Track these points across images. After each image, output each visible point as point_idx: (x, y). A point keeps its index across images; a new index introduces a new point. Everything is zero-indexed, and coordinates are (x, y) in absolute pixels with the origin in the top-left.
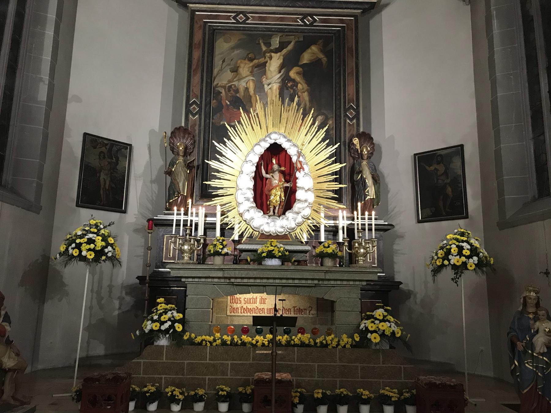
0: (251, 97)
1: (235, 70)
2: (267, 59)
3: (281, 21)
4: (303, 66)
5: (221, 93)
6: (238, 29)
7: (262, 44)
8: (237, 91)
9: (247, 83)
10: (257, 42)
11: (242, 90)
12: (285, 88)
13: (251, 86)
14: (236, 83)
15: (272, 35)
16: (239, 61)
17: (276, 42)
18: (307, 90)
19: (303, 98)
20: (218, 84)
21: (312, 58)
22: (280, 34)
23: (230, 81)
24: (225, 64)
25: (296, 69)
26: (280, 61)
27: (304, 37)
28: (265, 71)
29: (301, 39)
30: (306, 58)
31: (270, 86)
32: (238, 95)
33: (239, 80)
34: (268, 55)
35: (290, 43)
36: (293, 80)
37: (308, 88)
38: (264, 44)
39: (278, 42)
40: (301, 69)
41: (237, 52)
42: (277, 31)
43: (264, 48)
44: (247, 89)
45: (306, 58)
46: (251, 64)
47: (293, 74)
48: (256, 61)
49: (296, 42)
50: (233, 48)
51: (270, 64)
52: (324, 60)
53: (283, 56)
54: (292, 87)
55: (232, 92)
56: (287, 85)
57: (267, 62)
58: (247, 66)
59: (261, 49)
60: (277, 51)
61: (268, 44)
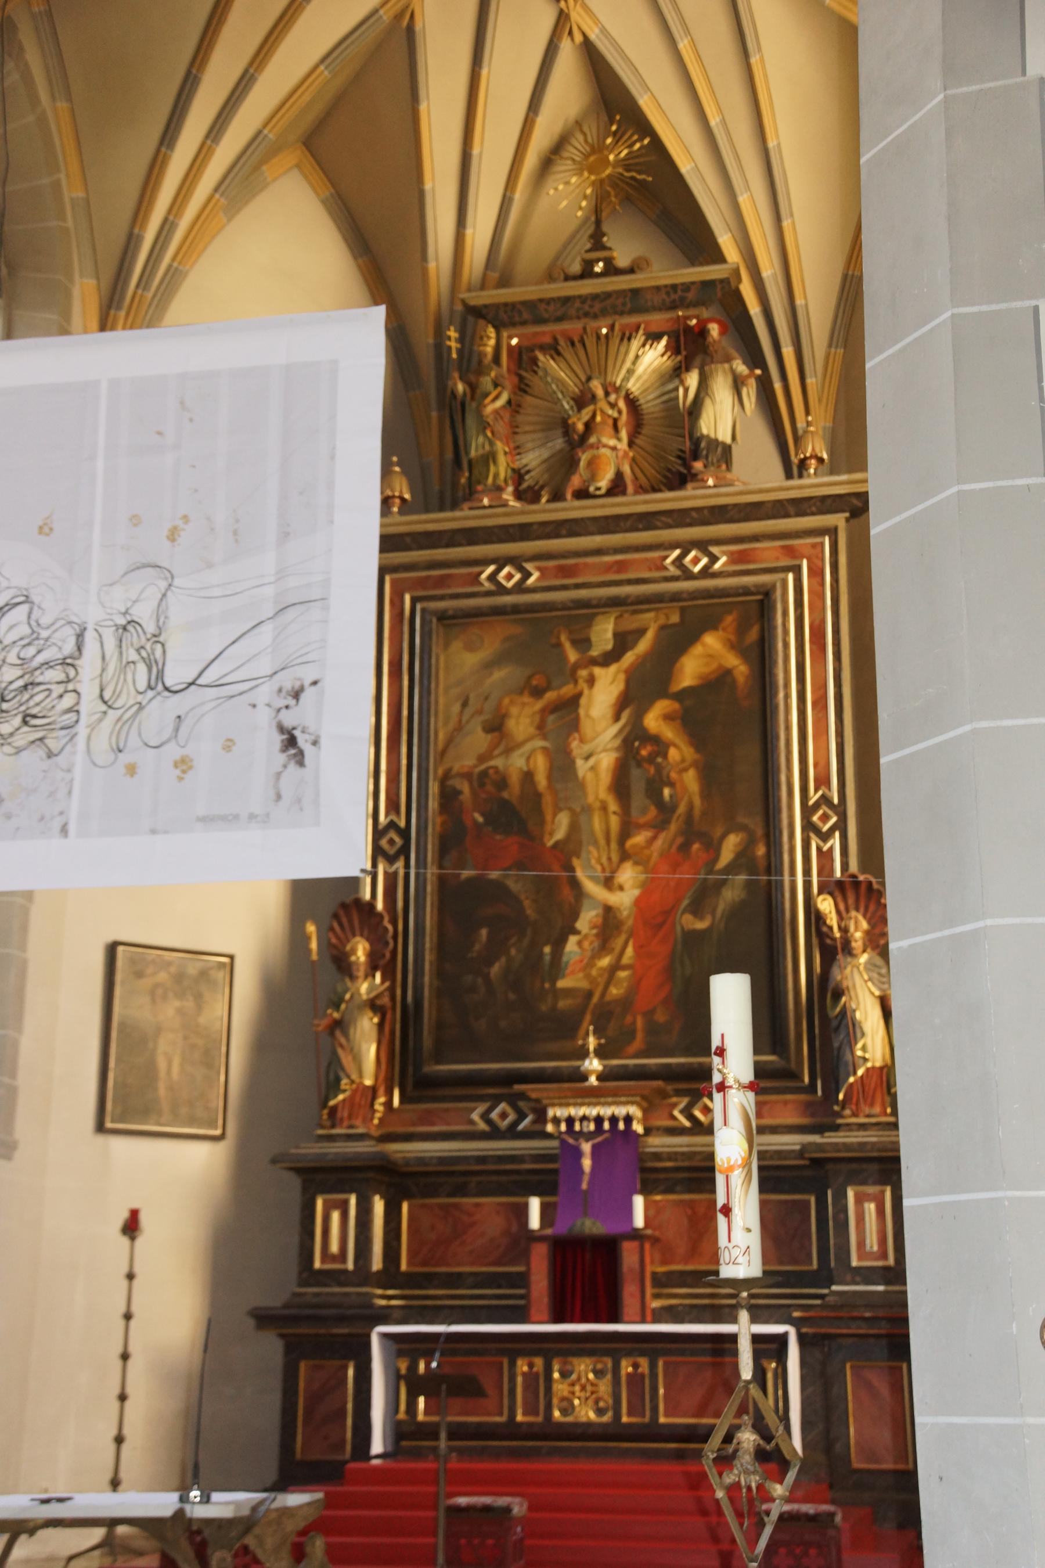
0: (539, 796)
1: (496, 726)
2: (582, 685)
3: (618, 571)
5: (460, 792)
6: (498, 611)
7: (567, 645)
8: (502, 782)
9: (528, 759)
10: (554, 641)
11: (515, 779)
12: (633, 763)
13: (541, 765)
14: (498, 762)
15: (595, 615)
16: (506, 701)
17: (604, 633)
18: (695, 764)
19: (685, 789)
20: (450, 769)
21: (706, 670)
22: (615, 612)
23: (482, 758)
24: (469, 711)
25: (662, 706)
26: (618, 687)
27: (683, 610)
28: (577, 719)
29: (675, 618)
30: (690, 670)
31: (591, 762)
32: (505, 795)
33: (508, 751)
34: (583, 673)
35: (641, 632)
36: (655, 740)
37: (696, 756)
38: (575, 643)
39: (610, 635)
40: (676, 706)
41: (499, 675)
42: (606, 605)
43: (573, 656)
44: (528, 776)
45: (690, 670)
46: (539, 705)
47: (653, 721)
48: (550, 696)
49: (663, 628)
50: (488, 666)
51: (590, 698)
52: (740, 668)
53: (626, 671)
54: (651, 759)
55: (489, 788)
56: (638, 752)
57: (579, 695)
58: (528, 711)
59: (563, 657)
61: (583, 643)
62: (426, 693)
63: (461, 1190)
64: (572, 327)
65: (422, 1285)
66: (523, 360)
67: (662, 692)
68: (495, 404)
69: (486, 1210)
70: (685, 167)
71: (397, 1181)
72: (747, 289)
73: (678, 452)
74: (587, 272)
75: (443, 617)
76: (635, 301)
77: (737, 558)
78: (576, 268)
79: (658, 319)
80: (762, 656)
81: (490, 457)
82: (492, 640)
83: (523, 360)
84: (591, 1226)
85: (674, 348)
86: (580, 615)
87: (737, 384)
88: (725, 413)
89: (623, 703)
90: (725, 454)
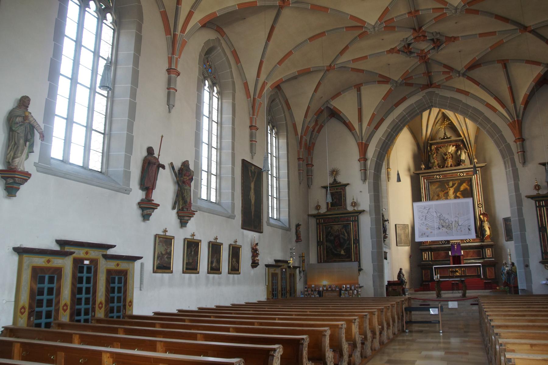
4: (461, 191)
17: (451, 184)
30: (462, 188)
45: (462, 188)
47: (458, 194)
52: (468, 188)
60: (452, 187)
61: (448, 185)
64: (443, 145)
65: (436, 262)
66: (437, 149)
68: (435, 156)
69: (442, 253)
71: (431, 250)
72: (464, 140)
73: (458, 162)
74: (444, 138)
75: (430, 182)
76: (451, 142)
78: (442, 137)
79: (454, 143)
80: (471, 186)
81: (435, 162)
83: (437, 149)
84: (457, 254)
85: (456, 147)
87: (465, 152)
88: (464, 156)
89: (454, 192)
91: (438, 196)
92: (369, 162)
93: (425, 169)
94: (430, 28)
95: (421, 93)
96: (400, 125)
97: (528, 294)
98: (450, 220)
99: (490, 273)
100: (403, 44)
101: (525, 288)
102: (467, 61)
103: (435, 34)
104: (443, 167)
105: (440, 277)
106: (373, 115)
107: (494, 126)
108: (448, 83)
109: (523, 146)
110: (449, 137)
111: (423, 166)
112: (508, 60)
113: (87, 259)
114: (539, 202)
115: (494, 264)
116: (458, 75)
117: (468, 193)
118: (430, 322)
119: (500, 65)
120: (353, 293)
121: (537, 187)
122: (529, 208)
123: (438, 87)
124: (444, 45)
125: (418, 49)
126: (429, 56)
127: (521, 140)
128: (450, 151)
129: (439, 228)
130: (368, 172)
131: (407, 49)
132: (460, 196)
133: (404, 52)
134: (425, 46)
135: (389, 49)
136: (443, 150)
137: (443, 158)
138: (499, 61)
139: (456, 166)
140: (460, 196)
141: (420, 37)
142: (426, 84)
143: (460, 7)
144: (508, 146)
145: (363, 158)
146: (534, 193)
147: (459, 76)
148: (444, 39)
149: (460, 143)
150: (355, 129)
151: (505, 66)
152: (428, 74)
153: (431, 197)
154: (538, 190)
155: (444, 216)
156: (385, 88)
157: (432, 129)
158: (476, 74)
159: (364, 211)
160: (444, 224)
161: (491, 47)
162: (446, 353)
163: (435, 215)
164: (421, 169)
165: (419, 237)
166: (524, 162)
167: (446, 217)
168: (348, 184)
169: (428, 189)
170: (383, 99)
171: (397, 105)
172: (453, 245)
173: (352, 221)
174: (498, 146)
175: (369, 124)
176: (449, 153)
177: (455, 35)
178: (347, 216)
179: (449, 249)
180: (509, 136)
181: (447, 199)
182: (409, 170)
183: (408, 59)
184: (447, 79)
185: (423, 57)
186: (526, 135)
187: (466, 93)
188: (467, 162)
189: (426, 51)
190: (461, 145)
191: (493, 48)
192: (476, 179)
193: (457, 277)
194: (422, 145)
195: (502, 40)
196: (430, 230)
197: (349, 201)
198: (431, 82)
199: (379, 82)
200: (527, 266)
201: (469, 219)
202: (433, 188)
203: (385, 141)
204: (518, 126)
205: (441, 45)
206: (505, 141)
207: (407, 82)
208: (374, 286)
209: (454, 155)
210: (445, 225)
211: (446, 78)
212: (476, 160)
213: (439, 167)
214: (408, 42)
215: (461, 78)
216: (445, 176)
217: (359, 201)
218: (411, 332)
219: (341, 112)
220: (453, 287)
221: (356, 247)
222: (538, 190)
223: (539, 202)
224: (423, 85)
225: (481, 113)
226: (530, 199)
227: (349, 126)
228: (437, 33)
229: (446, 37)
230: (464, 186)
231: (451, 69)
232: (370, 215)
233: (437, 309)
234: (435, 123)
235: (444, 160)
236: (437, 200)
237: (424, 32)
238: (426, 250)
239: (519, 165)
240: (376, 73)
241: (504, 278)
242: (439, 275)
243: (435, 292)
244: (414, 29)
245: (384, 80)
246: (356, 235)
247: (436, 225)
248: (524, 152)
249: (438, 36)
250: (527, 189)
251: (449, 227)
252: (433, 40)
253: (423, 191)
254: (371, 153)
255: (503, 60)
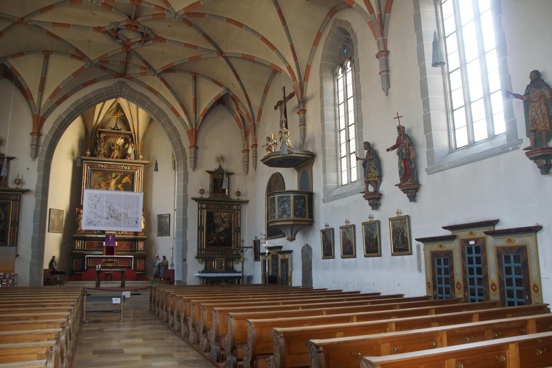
17: (114, 175)
30: (124, 181)
41: (100, 178)
45: (124, 181)
47: (119, 186)
52: (130, 181)
60: (114, 178)
61: (111, 176)
62: (91, 179)
63: (92, 240)
66: (105, 138)
67: (120, 183)
68: (102, 144)
70: (128, 118)
71: (85, 239)
72: (133, 135)
73: (125, 155)
74: (114, 129)
75: (93, 170)
76: (120, 134)
77: (131, 168)
79: (123, 136)
80: (133, 180)
81: (101, 151)
82: (99, 174)
84: (111, 245)
85: (125, 140)
86: (111, 173)
87: (132, 147)
88: (130, 151)
89: (115, 184)
90: (130, 155)
91: (99, 185)
92: (43, 139)
93: (89, 156)
94: (145, 22)
95: (112, 80)
96: (84, 107)
97: (183, 285)
98: (109, 211)
99: (140, 265)
100: (113, 27)
101: (181, 279)
102: (166, 64)
103: (146, 29)
104: (108, 157)
105: (102, 267)
106: (58, 90)
107: (174, 128)
108: (141, 79)
109: (195, 153)
110: (119, 128)
111: (89, 153)
112: (199, 74)
113: (471, 240)
114: (202, 204)
115: (145, 257)
116: (153, 73)
117: (129, 187)
118: (116, 310)
119: (191, 77)
120: (7, 282)
121: (202, 191)
122: (193, 207)
123: (131, 79)
124: (151, 42)
125: (125, 37)
126: (133, 47)
127: (195, 147)
128: (118, 143)
129: (108, 218)
130: (40, 149)
131: (114, 33)
132: (121, 188)
133: (110, 35)
134: (132, 36)
135: (96, 26)
136: (112, 140)
137: (110, 148)
138: (191, 73)
139: (121, 158)
140: (121, 188)
141: (132, 26)
142: (120, 72)
143: (180, 14)
144: (183, 150)
145: (37, 132)
146: (199, 196)
147: (155, 75)
148: (153, 36)
149: (128, 137)
150: (33, 99)
151: (195, 79)
152: (126, 64)
153: (92, 185)
154: (202, 194)
155: (114, 206)
156: (78, 65)
157: (104, 117)
158: (170, 77)
159: (28, 191)
160: (113, 215)
161: (189, 58)
162: (144, 339)
163: (105, 204)
164: (86, 155)
165: (86, 225)
166: (194, 168)
167: (116, 207)
168: (14, 158)
169: (90, 177)
170: (72, 75)
171: (85, 85)
172: (108, 236)
173: (13, 200)
174: (175, 148)
175: (51, 97)
176: (117, 144)
177: (164, 37)
178: (6, 194)
179: (103, 239)
180: (186, 142)
181: (107, 189)
182: (73, 154)
183: (112, 42)
184: (142, 74)
185: (127, 46)
186: (199, 144)
187: (156, 93)
188: (133, 156)
189: (132, 41)
190: (129, 139)
191: (191, 59)
192: (139, 174)
193: (112, 267)
194: (90, 130)
195: (201, 56)
196: (98, 219)
197: (11, 178)
198: (125, 72)
199: (73, 56)
200: (185, 260)
201: (137, 213)
202: (96, 176)
203: (65, 119)
204: (194, 134)
205: (148, 41)
206: (182, 145)
207: (103, 65)
208: (30, 275)
209: (121, 148)
210: (114, 216)
211: (141, 73)
212: (141, 157)
213: (105, 156)
214: (119, 26)
215: (156, 77)
216: (109, 166)
217: (25, 179)
218: (89, 322)
219: (20, 75)
220: (108, 277)
221: (14, 230)
222: (202, 194)
223: (202, 204)
224: (117, 73)
225: (165, 115)
226: (194, 201)
227: (26, 94)
228: (149, 29)
229: (156, 36)
230: (126, 179)
231: (149, 67)
232: (36, 197)
233: (119, 299)
234: (108, 112)
235: (111, 150)
236: (98, 189)
237: (138, 23)
238: (79, 239)
239: (190, 169)
240: (73, 46)
241: (155, 270)
242: (100, 265)
243: (94, 282)
244: (130, 17)
245: (80, 56)
246: (15, 216)
247: (105, 215)
248: (196, 158)
249: (149, 32)
250: (193, 192)
251: (117, 218)
252: (142, 33)
253: (84, 178)
254: (48, 127)
255: (195, 73)
